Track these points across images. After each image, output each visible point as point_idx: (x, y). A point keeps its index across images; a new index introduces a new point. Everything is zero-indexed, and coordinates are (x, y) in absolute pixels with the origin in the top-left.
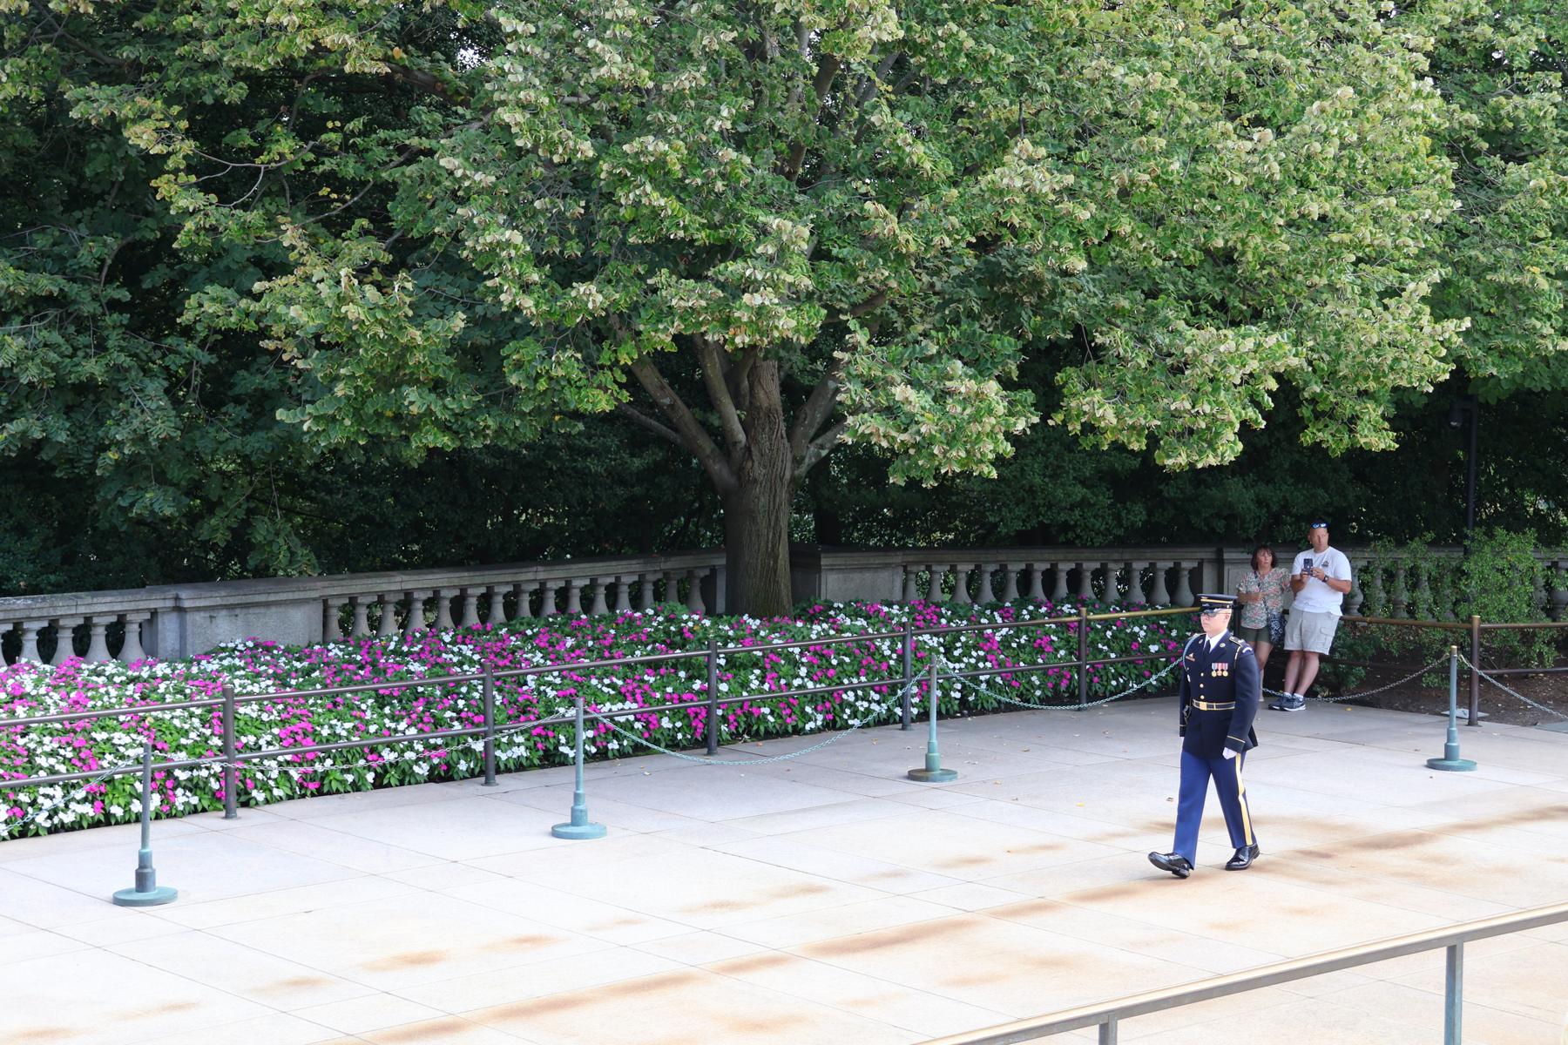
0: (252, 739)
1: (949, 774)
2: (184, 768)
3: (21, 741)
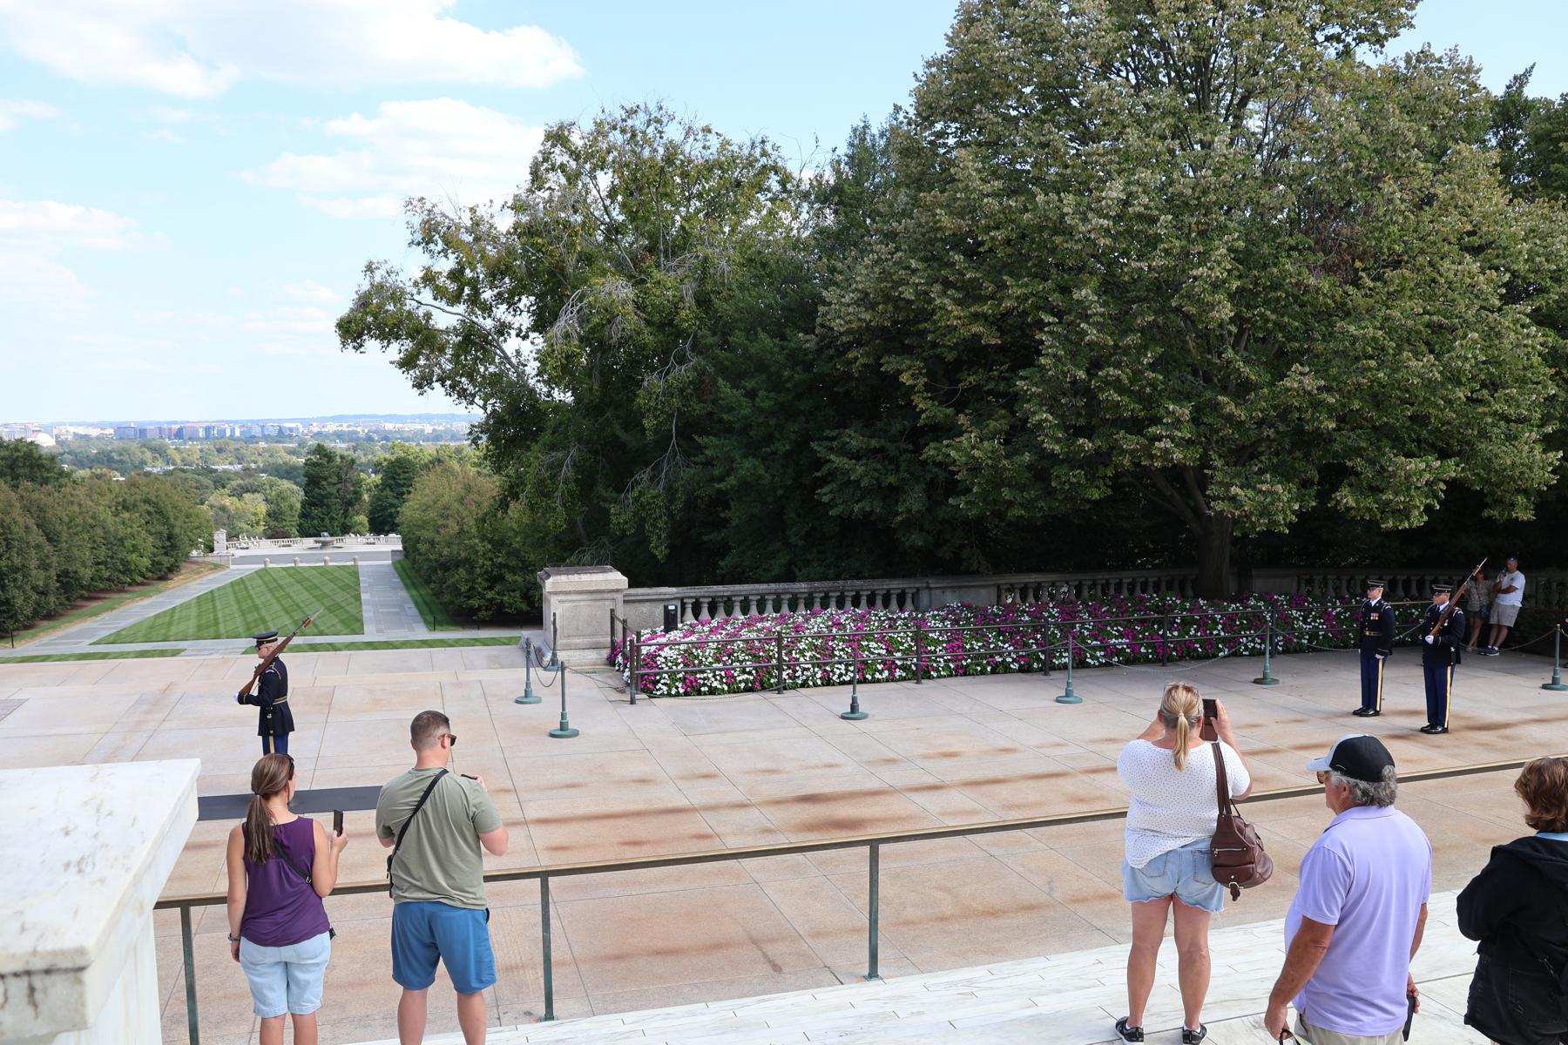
0: (933, 648)
1: (1275, 681)
2: (899, 659)
3: (830, 643)
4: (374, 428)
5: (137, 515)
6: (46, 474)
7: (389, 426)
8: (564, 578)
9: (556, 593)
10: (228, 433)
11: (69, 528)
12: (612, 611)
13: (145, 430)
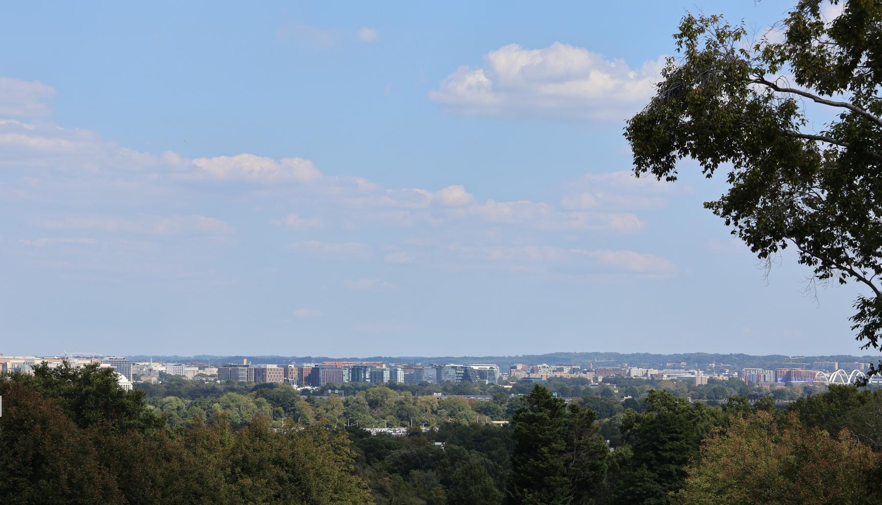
5: (264, 481)
6: (126, 421)
7: (636, 372)
11: (164, 496)
13: (264, 370)
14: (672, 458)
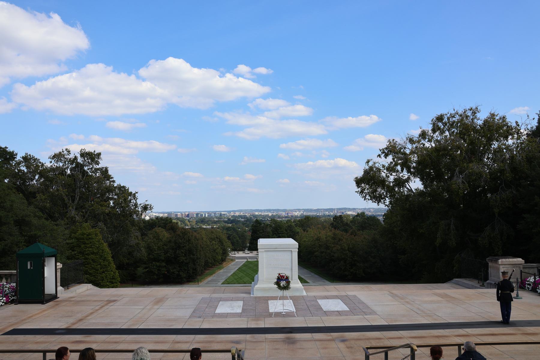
4: (252, 214)
7: (257, 213)
8: (504, 260)
9: (502, 265)
10: (204, 215)
12: (521, 271)
14: (280, 233)
